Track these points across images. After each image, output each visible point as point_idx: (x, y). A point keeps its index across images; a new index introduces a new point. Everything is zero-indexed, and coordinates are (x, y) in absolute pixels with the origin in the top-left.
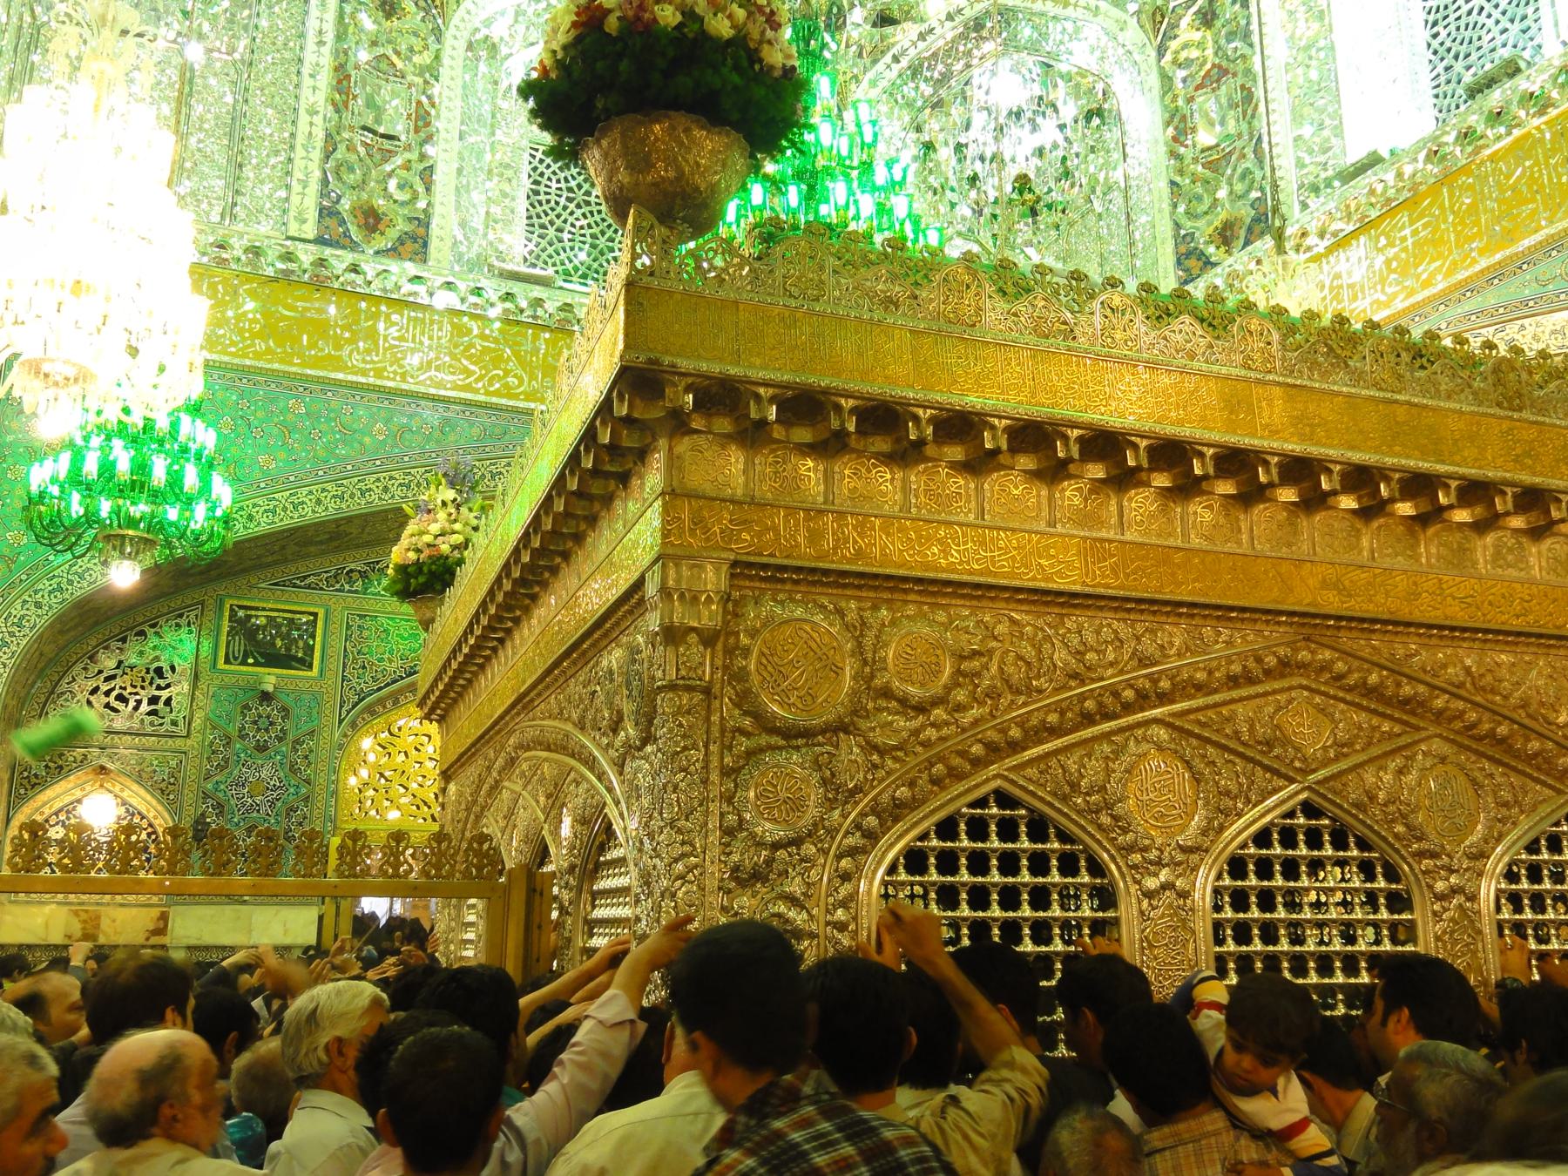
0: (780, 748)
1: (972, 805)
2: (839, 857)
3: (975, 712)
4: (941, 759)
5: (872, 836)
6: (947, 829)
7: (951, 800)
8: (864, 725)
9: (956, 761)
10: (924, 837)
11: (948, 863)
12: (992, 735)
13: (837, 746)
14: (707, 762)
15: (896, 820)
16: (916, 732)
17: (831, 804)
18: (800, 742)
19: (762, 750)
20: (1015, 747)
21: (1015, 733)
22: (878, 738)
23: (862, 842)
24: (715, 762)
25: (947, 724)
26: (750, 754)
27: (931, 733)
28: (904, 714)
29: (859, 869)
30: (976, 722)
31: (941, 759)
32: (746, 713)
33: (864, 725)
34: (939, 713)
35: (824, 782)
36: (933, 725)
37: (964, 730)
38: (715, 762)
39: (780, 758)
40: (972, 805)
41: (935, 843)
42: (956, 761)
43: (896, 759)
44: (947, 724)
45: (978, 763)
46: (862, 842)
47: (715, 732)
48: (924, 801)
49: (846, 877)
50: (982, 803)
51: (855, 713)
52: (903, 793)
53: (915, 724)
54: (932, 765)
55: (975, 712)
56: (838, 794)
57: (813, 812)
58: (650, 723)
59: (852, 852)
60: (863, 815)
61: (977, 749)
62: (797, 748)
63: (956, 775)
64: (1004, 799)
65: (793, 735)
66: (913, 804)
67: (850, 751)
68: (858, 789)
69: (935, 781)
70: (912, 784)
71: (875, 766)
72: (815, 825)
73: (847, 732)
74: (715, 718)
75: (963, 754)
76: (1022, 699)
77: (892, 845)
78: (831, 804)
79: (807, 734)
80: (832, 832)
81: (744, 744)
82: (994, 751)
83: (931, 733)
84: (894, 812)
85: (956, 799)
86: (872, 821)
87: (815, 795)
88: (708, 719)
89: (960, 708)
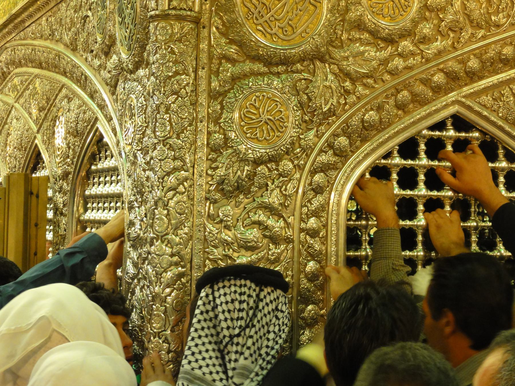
0: (262, 74)
1: (432, 128)
2: (313, 172)
3: (438, 44)
4: (407, 86)
5: (343, 155)
6: (408, 149)
7: (414, 123)
8: (338, 54)
9: (420, 88)
10: (388, 155)
11: (408, 178)
12: (454, 66)
13: (314, 74)
14: (196, 86)
15: (364, 140)
16: (385, 62)
17: (306, 125)
18: (281, 69)
19: (246, 76)
20: (473, 76)
21: (474, 64)
22: (352, 66)
23: (333, 159)
24: (203, 86)
25: (413, 54)
26: (235, 79)
27: (398, 63)
28: (376, 45)
29: (330, 184)
30: (440, 53)
31: (407, 86)
32: (232, 42)
33: (338, 54)
34: (406, 44)
35: (301, 105)
36: (400, 55)
37: (428, 61)
38: (203, 86)
39: (263, 82)
40: (432, 128)
41: (397, 160)
42: (420, 88)
43: (366, 86)
44: (413, 54)
45: (439, 90)
46: (333, 159)
47: (204, 58)
48: (390, 124)
49: (318, 190)
50: (440, 126)
51: (331, 43)
52: (372, 116)
53: (384, 54)
54: (398, 92)
55: (438, 44)
56: (313, 116)
57: (291, 132)
58: (143, 48)
59: (325, 168)
60: (335, 135)
61: (439, 78)
62: (278, 74)
63: (419, 101)
64: (460, 123)
65: (275, 63)
66: (380, 126)
67: (325, 78)
68: (332, 112)
69: (401, 106)
70: (379, 109)
71: (347, 92)
72: (292, 143)
73: (323, 60)
74: (203, 46)
75: (426, 82)
76: (482, 33)
77: (359, 163)
78: (306, 125)
79: (286, 61)
80: (307, 150)
81: (229, 70)
82: (454, 79)
83: (398, 63)
84: (365, 132)
85: (417, 123)
86: (343, 141)
87: (293, 116)
88: (197, 47)
89: (425, 40)
